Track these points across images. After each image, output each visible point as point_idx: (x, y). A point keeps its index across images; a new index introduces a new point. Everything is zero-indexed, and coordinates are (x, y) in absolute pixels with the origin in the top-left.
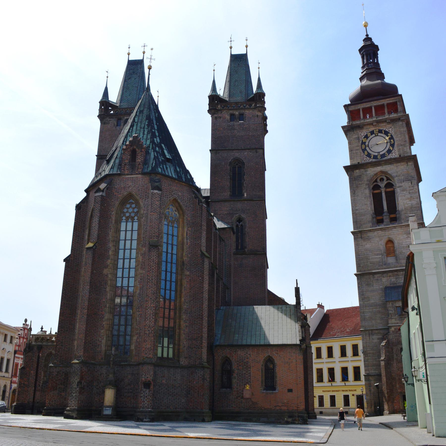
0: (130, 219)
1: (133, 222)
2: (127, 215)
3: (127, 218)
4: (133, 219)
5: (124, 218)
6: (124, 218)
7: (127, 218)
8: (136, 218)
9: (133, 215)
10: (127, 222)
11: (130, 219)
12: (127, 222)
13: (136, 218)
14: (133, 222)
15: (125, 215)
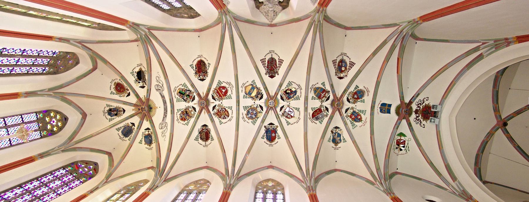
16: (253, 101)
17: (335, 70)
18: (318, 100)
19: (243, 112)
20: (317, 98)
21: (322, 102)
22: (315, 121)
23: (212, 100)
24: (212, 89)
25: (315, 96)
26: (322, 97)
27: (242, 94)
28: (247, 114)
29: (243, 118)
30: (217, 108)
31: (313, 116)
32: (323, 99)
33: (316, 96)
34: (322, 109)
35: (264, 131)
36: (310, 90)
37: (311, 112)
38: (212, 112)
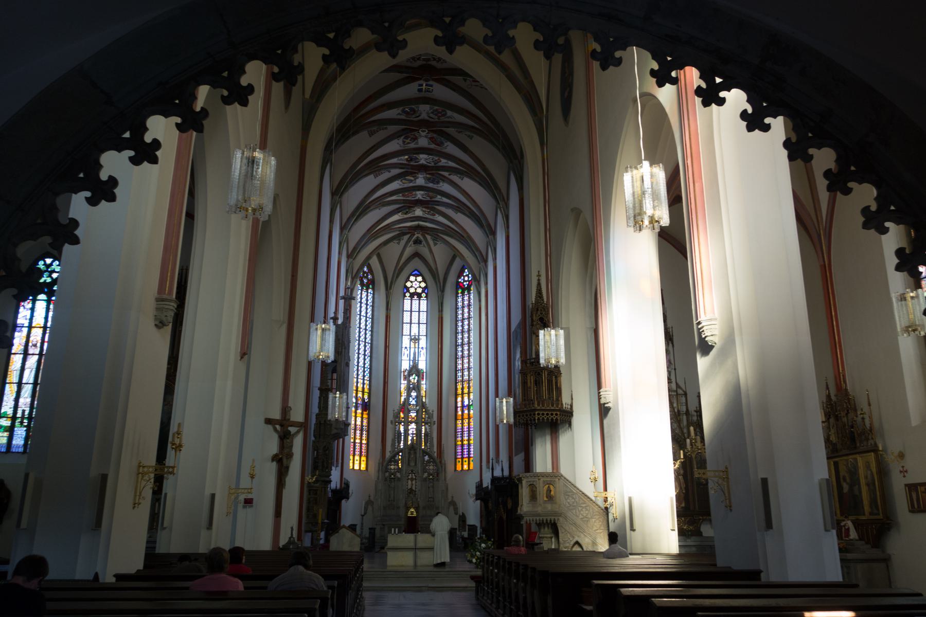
0: (416, 297)
1: (419, 300)
2: (412, 290)
3: (412, 295)
4: (419, 296)
5: (408, 294)
6: (408, 294)
7: (412, 295)
8: (424, 295)
9: (419, 290)
10: (411, 300)
11: (416, 297)
12: (411, 300)
13: (424, 295)
14: (419, 300)
15: (408, 291)
16: (420, 178)
17: (380, 130)
18: (419, 140)
19: (431, 185)
20: (416, 141)
21: (421, 136)
22: (445, 145)
23: (417, 198)
24: (405, 198)
25: (414, 143)
26: (414, 137)
27: (411, 184)
28: (434, 184)
29: (438, 187)
30: (424, 196)
31: (438, 145)
32: (417, 135)
33: (413, 142)
34: (429, 136)
35: (455, 176)
36: (407, 148)
37: (433, 146)
38: (429, 199)
